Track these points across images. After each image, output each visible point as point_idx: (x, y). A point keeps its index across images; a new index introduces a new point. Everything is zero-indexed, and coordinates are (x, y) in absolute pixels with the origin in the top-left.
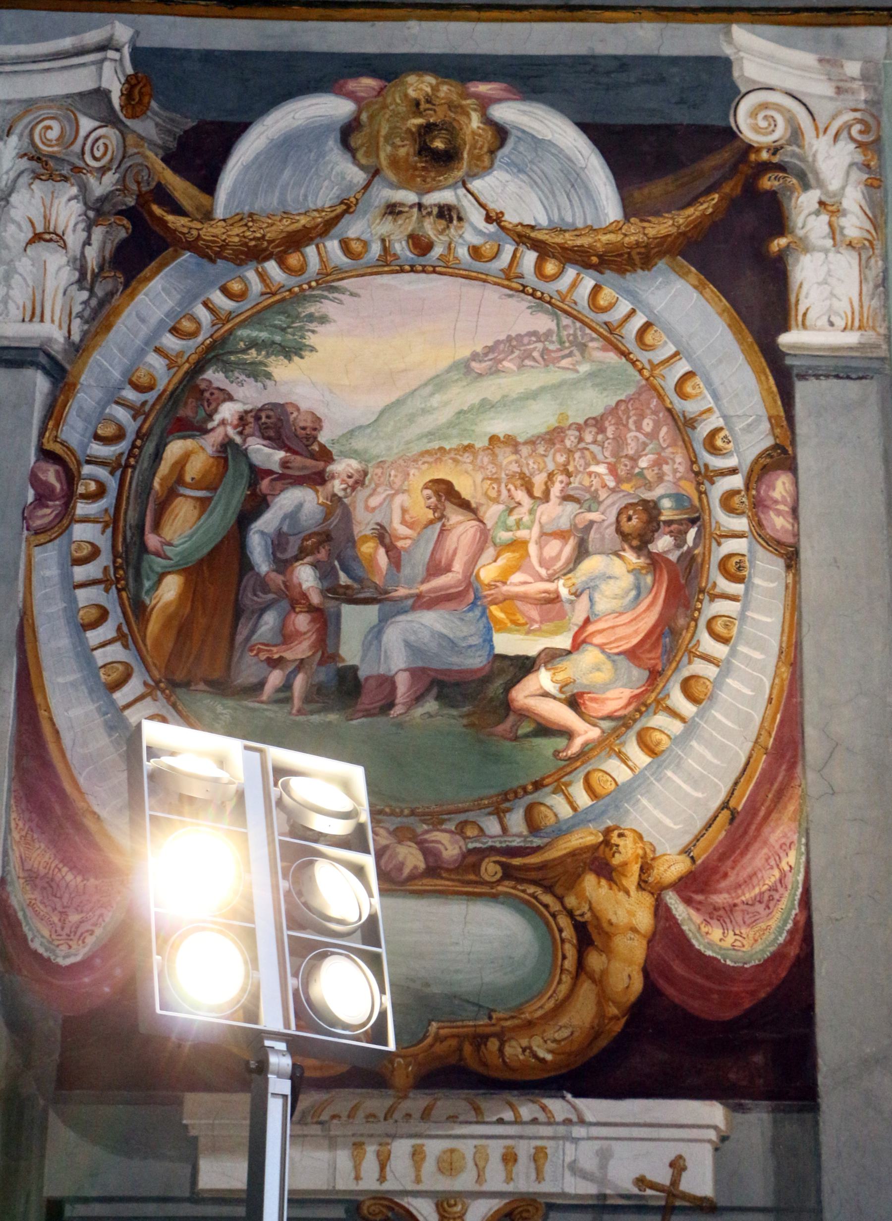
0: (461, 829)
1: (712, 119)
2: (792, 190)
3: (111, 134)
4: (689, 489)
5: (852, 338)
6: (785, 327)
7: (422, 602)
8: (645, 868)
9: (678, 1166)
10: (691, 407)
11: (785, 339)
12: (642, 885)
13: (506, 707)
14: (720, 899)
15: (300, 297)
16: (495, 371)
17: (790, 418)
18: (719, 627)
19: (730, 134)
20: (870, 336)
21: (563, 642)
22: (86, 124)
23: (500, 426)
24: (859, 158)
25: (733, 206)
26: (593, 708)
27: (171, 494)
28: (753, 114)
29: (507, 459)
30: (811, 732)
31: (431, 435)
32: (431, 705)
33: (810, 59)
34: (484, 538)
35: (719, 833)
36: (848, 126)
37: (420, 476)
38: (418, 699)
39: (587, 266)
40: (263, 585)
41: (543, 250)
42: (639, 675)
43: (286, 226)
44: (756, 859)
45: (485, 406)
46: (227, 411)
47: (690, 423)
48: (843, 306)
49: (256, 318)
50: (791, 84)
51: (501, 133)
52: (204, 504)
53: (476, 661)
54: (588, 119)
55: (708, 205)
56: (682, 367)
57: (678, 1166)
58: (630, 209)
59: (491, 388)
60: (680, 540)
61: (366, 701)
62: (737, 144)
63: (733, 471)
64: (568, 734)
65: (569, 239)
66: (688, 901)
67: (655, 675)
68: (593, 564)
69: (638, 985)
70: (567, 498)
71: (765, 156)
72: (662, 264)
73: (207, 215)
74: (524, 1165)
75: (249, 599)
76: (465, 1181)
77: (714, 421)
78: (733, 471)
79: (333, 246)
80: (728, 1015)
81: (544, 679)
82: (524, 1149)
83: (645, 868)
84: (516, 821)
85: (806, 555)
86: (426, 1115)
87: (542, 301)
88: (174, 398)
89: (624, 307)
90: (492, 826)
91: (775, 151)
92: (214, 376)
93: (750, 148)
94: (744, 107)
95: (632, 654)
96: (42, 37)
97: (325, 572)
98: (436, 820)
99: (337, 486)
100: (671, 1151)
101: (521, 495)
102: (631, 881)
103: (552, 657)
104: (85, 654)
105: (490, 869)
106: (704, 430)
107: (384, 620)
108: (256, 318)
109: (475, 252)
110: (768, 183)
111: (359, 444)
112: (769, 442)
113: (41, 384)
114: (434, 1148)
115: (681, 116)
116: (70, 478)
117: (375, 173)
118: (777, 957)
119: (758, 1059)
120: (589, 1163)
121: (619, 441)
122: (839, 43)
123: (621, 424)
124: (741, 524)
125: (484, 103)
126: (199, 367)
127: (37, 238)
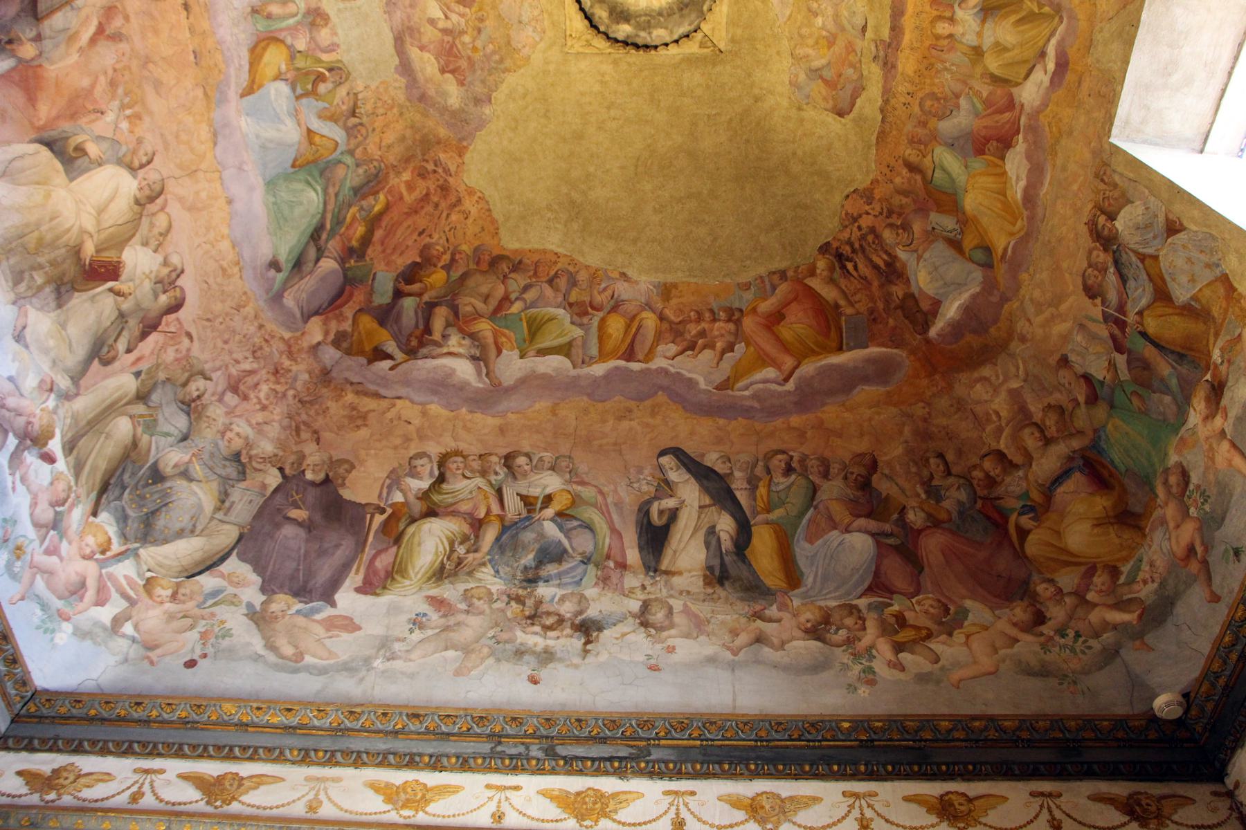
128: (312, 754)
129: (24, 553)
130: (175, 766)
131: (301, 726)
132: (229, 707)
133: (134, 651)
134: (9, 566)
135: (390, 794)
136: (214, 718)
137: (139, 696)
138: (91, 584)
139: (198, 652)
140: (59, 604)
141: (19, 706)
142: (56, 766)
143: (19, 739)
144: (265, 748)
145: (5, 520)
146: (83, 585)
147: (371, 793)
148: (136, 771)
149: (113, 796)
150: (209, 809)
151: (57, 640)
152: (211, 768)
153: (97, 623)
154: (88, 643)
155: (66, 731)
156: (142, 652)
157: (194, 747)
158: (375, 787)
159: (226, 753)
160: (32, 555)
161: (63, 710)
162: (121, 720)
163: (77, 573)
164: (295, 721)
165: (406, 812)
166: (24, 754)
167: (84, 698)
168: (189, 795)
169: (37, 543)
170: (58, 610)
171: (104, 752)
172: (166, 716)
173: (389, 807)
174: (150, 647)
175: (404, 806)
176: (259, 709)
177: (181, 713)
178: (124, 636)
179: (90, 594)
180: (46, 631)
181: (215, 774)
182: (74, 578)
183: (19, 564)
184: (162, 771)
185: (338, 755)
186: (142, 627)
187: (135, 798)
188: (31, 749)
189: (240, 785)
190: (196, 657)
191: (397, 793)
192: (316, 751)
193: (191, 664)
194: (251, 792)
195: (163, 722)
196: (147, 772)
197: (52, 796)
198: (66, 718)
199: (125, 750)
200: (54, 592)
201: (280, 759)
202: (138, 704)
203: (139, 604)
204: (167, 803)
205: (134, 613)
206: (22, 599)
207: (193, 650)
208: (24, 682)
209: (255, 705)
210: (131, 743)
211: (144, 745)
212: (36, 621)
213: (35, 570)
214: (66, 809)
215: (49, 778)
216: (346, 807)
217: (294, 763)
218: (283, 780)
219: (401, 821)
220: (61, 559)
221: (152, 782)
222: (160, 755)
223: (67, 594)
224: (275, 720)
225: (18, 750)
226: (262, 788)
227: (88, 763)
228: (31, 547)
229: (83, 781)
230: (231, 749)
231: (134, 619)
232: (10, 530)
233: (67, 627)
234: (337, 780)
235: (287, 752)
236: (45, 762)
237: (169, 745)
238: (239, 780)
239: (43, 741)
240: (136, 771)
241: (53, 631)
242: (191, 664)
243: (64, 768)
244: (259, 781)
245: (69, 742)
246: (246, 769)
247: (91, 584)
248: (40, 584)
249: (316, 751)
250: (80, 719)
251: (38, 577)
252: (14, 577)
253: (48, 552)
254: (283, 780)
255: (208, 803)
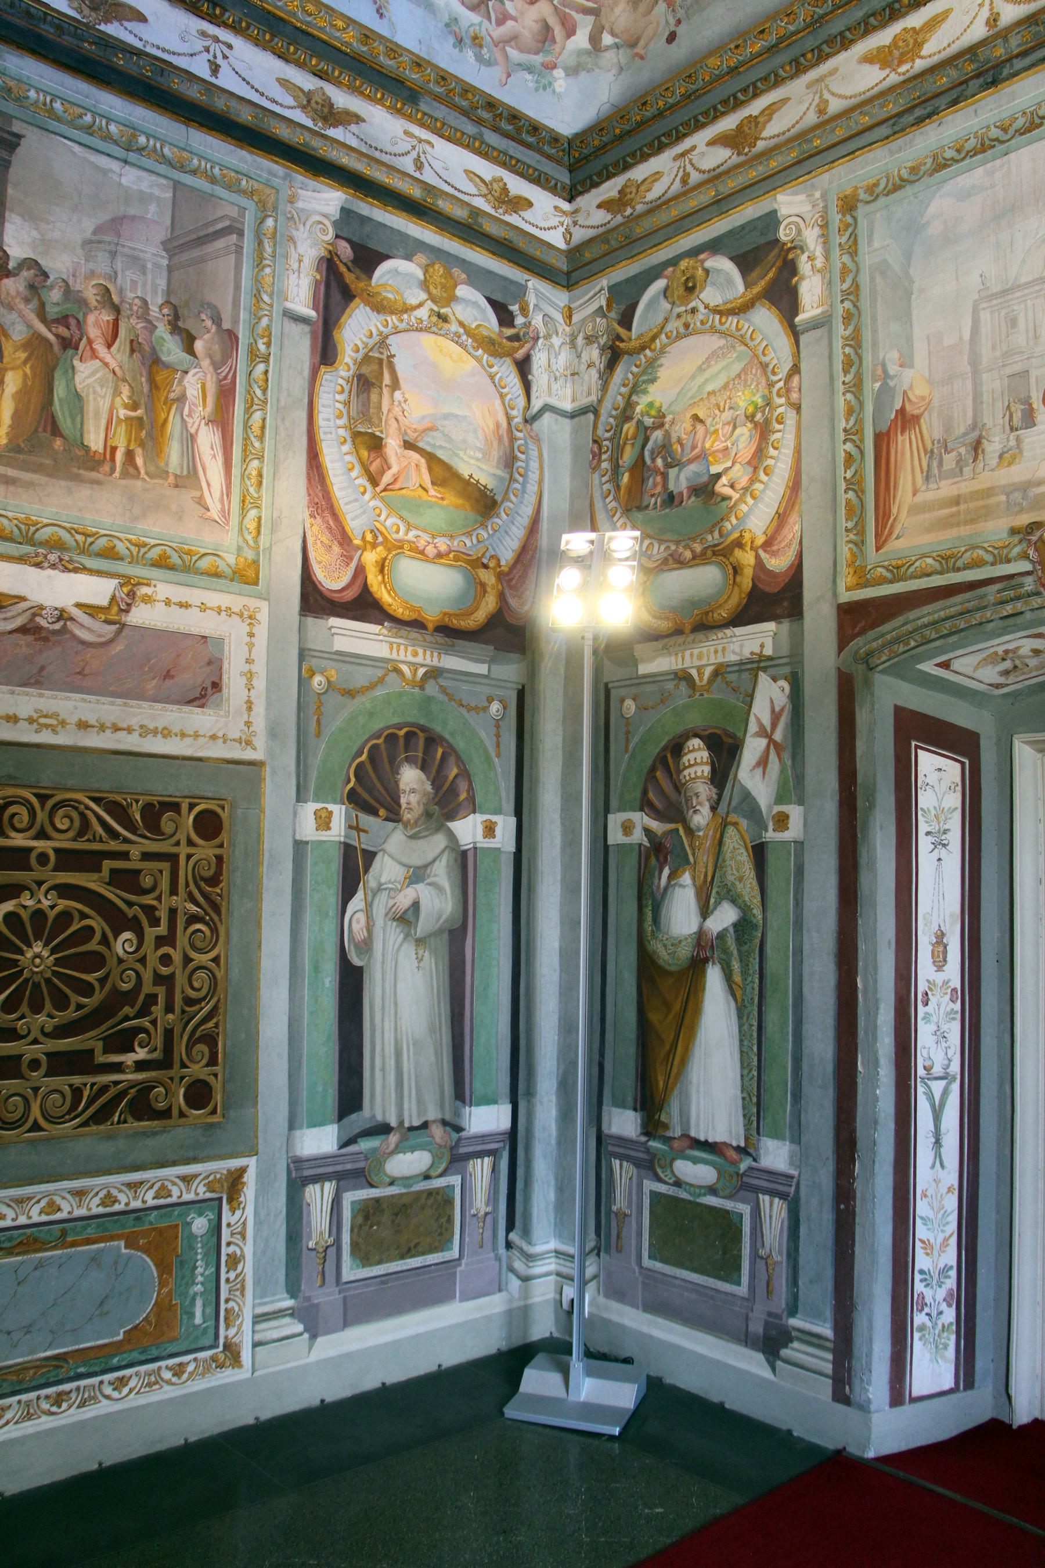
0: (701, 542)
1: (770, 237)
2: (798, 256)
3: (604, 320)
4: (766, 392)
5: (819, 311)
6: (797, 315)
7: (690, 461)
8: (752, 542)
9: (762, 646)
10: (764, 359)
11: (797, 319)
12: (752, 548)
13: (713, 493)
14: (775, 548)
15: (655, 359)
16: (709, 366)
17: (799, 352)
18: (775, 444)
19: (777, 241)
20: (826, 307)
21: (729, 464)
22: (598, 320)
23: (710, 388)
24: (821, 232)
25: (780, 270)
26: (738, 486)
27: (625, 444)
28: (785, 229)
29: (713, 399)
30: (803, 477)
31: (692, 398)
32: (693, 499)
33: (802, 197)
34: (707, 431)
35: (775, 523)
36: (817, 220)
37: (689, 415)
38: (689, 497)
39: (736, 314)
40: (649, 468)
41: (721, 313)
42: (751, 470)
43: (651, 334)
44: (785, 531)
45: (707, 381)
46: (638, 409)
47: (767, 365)
48: (816, 298)
49: (644, 372)
50: (796, 211)
51: (707, 272)
52: (633, 444)
53: (705, 479)
54: (734, 254)
55: (771, 275)
56: (765, 343)
57: (762, 646)
58: (747, 286)
59: (707, 375)
60: (763, 412)
61: (676, 502)
62: (780, 245)
63: (780, 380)
64: (730, 498)
65: (729, 306)
66: (765, 551)
67: (756, 468)
68: (738, 431)
69: (750, 585)
70: (731, 408)
71: (789, 245)
72: (757, 304)
73: (630, 339)
74: (720, 653)
75: (646, 475)
76: (704, 662)
77: (775, 361)
78: (780, 380)
79: (663, 336)
80: (776, 590)
81: (724, 480)
82: (720, 648)
83: (752, 542)
84: (716, 534)
85: (803, 406)
86: (693, 642)
87: (723, 334)
88: (625, 410)
89: (747, 326)
90: (710, 538)
91: (792, 242)
92: (634, 398)
93: (785, 244)
94: (782, 227)
95: (749, 463)
96: (584, 295)
97: (664, 459)
98: (693, 539)
99: (667, 426)
100: (759, 642)
101: (717, 412)
102: (748, 548)
103: (727, 470)
104: (605, 505)
105: (709, 553)
106: (771, 367)
107: (680, 471)
108: (644, 372)
109: (702, 323)
110: (790, 256)
111: (672, 409)
112: (791, 364)
113: (591, 416)
114: (696, 651)
115: (762, 241)
116: (600, 447)
117: (673, 304)
118: (792, 565)
119: (786, 604)
120: (737, 650)
121: (746, 381)
122: (813, 186)
123: (746, 374)
124: (782, 401)
125: (703, 261)
126: (630, 396)
127: (589, 366)
128: (802, 60)
129: (482, 38)
130: (700, 138)
131: (781, 40)
132: (713, 62)
133: (623, 56)
134: (479, 58)
135: (882, 58)
136: (707, 78)
137: (641, 97)
138: (553, 21)
139: (672, 21)
140: (539, 59)
141: (566, 158)
142: (619, 188)
143: (583, 183)
144: (760, 79)
145: (447, 25)
146: (547, 28)
147: (867, 68)
148: (675, 159)
149: (669, 188)
150: (742, 158)
151: (558, 90)
152: (728, 123)
153: (580, 53)
154: (583, 75)
155: (609, 158)
156: (629, 52)
157: (705, 114)
158: (868, 59)
159: (733, 103)
160: (490, 35)
161: (596, 143)
162: (642, 124)
163: (536, 22)
164: (773, 39)
165: (903, 69)
166: (594, 191)
167: (604, 125)
168: (722, 155)
169: (486, 22)
170: (542, 64)
171: (645, 157)
172: (670, 101)
173: (887, 71)
174: (633, 45)
175: (901, 62)
176: (737, 47)
177: (680, 90)
178: (608, 48)
179: (558, 31)
180: (545, 88)
181: (734, 127)
182: (536, 27)
183: (485, 50)
184: (694, 148)
185: (825, 47)
186: (617, 31)
187: (684, 181)
188: (595, 185)
189: (757, 124)
190: (673, 29)
191: (890, 53)
192: (803, 55)
193: (672, 38)
194: (768, 126)
195: (672, 106)
196: (683, 155)
197: (629, 211)
198: (603, 148)
199: (658, 147)
200: (528, 52)
201: (778, 82)
202: (644, 104)
203: (603, 9)
204: (709, 171)
205: (603, 22)
206: (509, 75)
207: (667, 22)
208: (555, 139)
209: (732, 46)
210: (658, 138)
211: (667, 135)
212: (531, 85)
213: (501, 45)
214: (640, 216)
215: (620, 199)
216: (848, 93)
217: (792, 78)
218: (788, 99)
219: (902, 78)
220: (515, 19)
221: (690, 160)
222: (685, 135)
223: (540, 45)
224: (757, 47)
225: (588, 191)
226: (775, 116)
227: (639, 172)
228: (483, 29)
229: (642, 188)
230: (735, 98)
231: (607, 26)
232: (457, 30)
233: (558, 73)
234: (833, 72)
235: (781, 72)
236: (610, 189)
237: (686, 124)
238: (753, 121)
239: (599, 174)
240: (675, 159)
241: (550, 84)
242: (672, 38)
243: (625, 186)
244: (770, 111)
245: (616, 165)
246: (755, 107)
247: (553, 21)
248: (513, 53)
249: (803, 55)
250: (613, 142)
251: (508, 49)
252: (489, 63)
253: (500, 22)
254: (788, 99)
255: (739, 154)
